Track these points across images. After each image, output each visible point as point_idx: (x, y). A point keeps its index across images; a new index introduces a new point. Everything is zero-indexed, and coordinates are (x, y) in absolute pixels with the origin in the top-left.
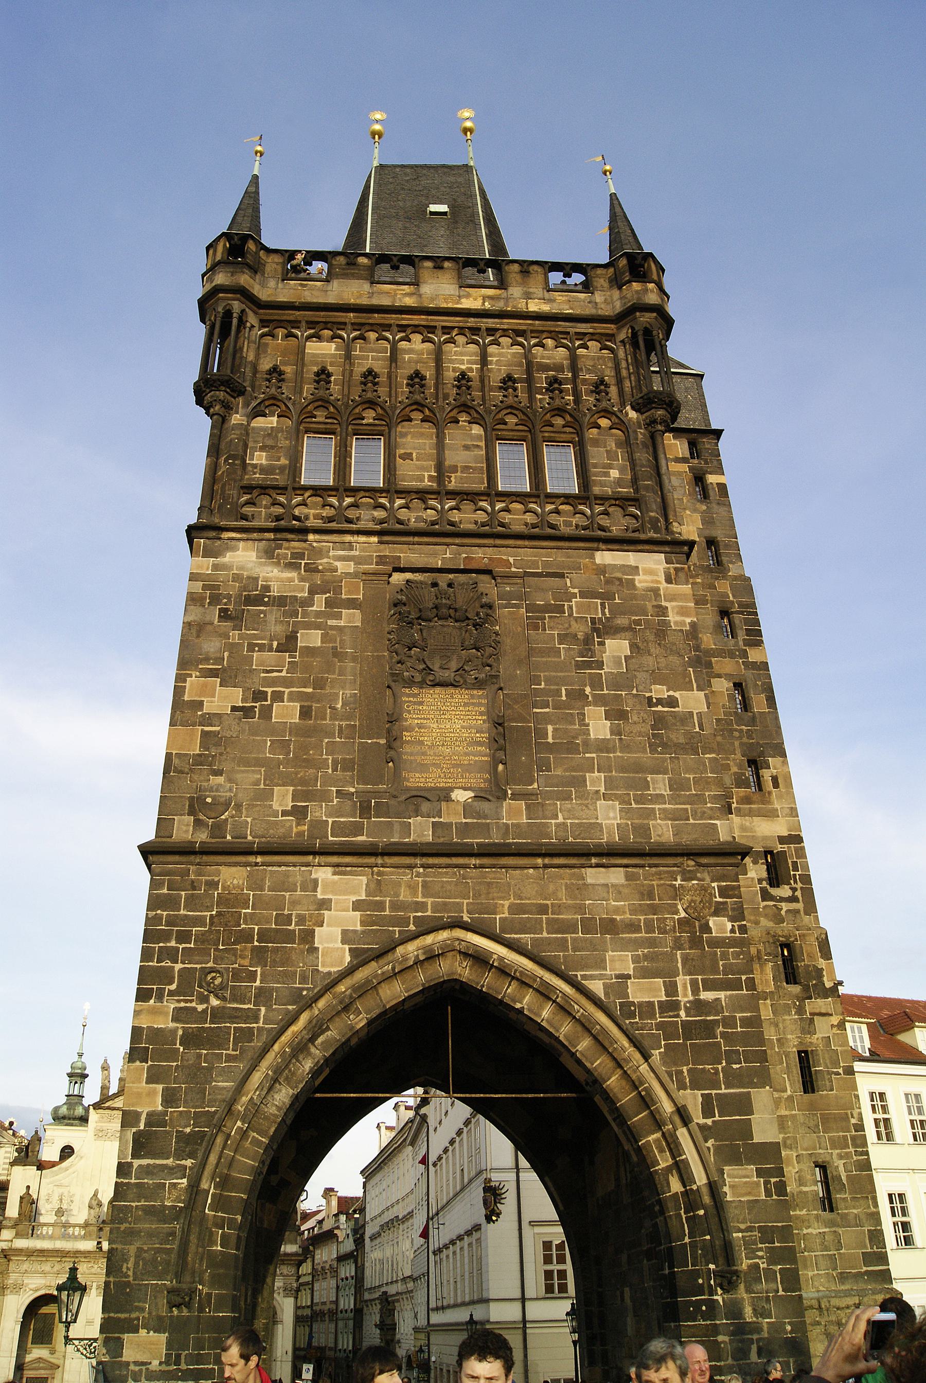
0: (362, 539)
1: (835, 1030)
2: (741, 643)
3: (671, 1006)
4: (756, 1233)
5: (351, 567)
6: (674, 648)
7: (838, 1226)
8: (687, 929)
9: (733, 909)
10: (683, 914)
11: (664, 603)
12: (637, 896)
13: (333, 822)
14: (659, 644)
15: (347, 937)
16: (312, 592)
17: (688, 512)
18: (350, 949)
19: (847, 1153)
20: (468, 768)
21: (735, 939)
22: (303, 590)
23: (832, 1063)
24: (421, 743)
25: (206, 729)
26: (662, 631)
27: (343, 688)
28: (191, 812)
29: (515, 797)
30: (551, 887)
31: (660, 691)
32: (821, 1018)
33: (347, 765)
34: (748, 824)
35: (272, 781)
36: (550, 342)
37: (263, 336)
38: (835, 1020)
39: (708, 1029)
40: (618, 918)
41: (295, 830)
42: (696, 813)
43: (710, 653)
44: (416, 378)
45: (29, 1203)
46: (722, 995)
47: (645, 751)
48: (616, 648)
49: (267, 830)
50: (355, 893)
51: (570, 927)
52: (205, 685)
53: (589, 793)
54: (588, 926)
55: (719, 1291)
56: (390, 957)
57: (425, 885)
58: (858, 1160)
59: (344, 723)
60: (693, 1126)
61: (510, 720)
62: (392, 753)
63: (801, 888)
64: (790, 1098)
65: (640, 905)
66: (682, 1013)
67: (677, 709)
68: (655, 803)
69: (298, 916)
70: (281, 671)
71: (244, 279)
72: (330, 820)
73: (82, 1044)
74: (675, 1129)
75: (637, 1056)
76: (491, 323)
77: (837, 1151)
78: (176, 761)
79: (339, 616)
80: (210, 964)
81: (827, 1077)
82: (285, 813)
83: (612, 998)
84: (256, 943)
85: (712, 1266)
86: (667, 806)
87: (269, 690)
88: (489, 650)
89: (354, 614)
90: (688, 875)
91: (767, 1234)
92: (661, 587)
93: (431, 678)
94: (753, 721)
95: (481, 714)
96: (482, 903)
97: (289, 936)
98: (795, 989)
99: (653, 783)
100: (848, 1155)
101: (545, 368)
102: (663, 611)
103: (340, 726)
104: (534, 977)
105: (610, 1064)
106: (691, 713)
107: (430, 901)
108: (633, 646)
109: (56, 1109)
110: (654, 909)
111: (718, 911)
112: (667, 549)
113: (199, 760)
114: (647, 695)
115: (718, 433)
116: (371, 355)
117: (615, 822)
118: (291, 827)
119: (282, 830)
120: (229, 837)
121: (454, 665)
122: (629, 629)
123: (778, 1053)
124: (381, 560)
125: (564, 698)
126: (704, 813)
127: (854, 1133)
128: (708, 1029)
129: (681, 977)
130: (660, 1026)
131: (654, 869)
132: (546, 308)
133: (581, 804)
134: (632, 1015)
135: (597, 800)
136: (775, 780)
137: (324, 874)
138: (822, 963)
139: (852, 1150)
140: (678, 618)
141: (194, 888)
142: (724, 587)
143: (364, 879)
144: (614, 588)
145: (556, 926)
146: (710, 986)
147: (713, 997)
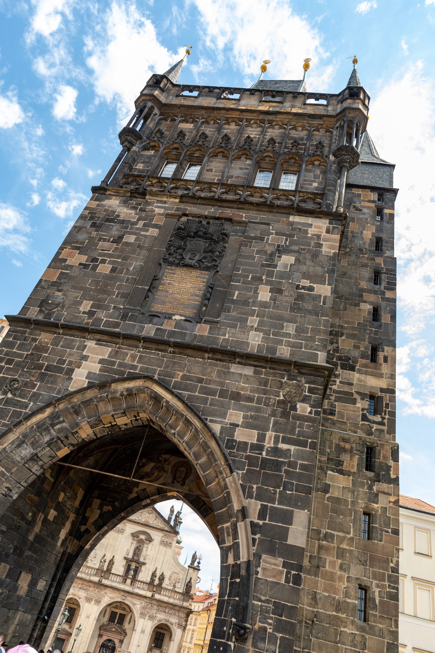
0: (172, 200)
1: (391, 504)
2: (382, 288)
3: (259, 448)
4: (271, 606)
5: (162, 211)
6: (321, 263)
7: (366, 633)
8: (282, 406)
9: (314, 401)
10: (282, 398)
11: (321, 242)
12: (257, 384)
13: (106, 320)
14: (312, 261)
15: (89, 375)
16: (139, 220)
17: (369, 225)
18: (89, 382)
19: (382, 585)
21: (310, 418)
22: (135, 218)
23: (385, 524)
24: (167, 291)
25: (63, 271)
26: (315, 255)
27: (136, 261)
28: (40, 306)
29: (206, 322)
30: (209, 370)
31: (306, 283)
32: (383, 495)
33: (124, 296)
34: (363, 378)
35: (84, 297)
37: (161, 119)
38: (392, 499)
39: (277, 465)
40: (242, 393)
41: (86, 321)
42: (307, 345)
43: (362, 290)
46: (292, 448)
47: (287, 311)
48: (287, 260)
49: (72, 319)
50: (102, 355)
51: (213, 393)
52: (71, 253)
53: (247, 326)
54: (223, 394)
55: (234, 640)
56: (107, 389)
57: (141, 357)
58: (390, 592)
59: (130, 277)
60: (248, 520)
61: (217, 287)
62: (149, 294)
63: (388, 418)
64: (352, 539)
65: (258, 388)
66: (264, 453)
67: (312, 293)
68: (284, 337)
69: (69, 361)
70: (109, 251)
72: (105, 319)
74: (237, 521)
75: (228, 471)
76: (271, 117)
77: (376, 582)
78: (43, 283)
79: (147, 230)
80: (16, 377)
81: (379, 532)
82: (84, 313)
83: (224, 435)
84: (43, 371)
85: (234, 620)
86: (291, 340)
87: (100, 258)
88: (217, 253)
89: (155, 231)
90: (292, 377)
91: (279, 609)
92: (322, 234)
93: (182, 262)
95: (203, 282)
96: (167, 372)
97: (60, 370)
98: (371, 474)
99: (286, 327)
100: (383, 587)
102: (320, 246)
103: (128, 278)
104: (182, 415)
105: (214, 475)
106: (320, 296)
107: (140, 365)
108: (297, 260)
110: (265, 392)
111: (304, 400)
112: (331, 218)
113: (54, 284)
114: (297, 283)
117: (257, 343)
118: (84, 320)
119: (79, 320)
120: (52, 320)
121: (197, 258)
122: (298, 252)
123: (350, 509)
124: (178, 209)
125: (249, 279)
126: (312, 346)
127: (390, 573)
128: (277, 465)
129: (270, 432)
130: (247, 457)
131: (272, 371)
132: (301, 111)
133: (241, 331)
134: (233, 447)
135: (251, 330)
136: (386, 359)
137: (91, 344)
138: (391, 463)
139: (387, 583)
140: (327, 250)
141: (25, 340)
142: (380, 260)
143: (110, 349)
144: (295, 233)
145: (205, 391)
146: (285, 441)
147: (286, 448)
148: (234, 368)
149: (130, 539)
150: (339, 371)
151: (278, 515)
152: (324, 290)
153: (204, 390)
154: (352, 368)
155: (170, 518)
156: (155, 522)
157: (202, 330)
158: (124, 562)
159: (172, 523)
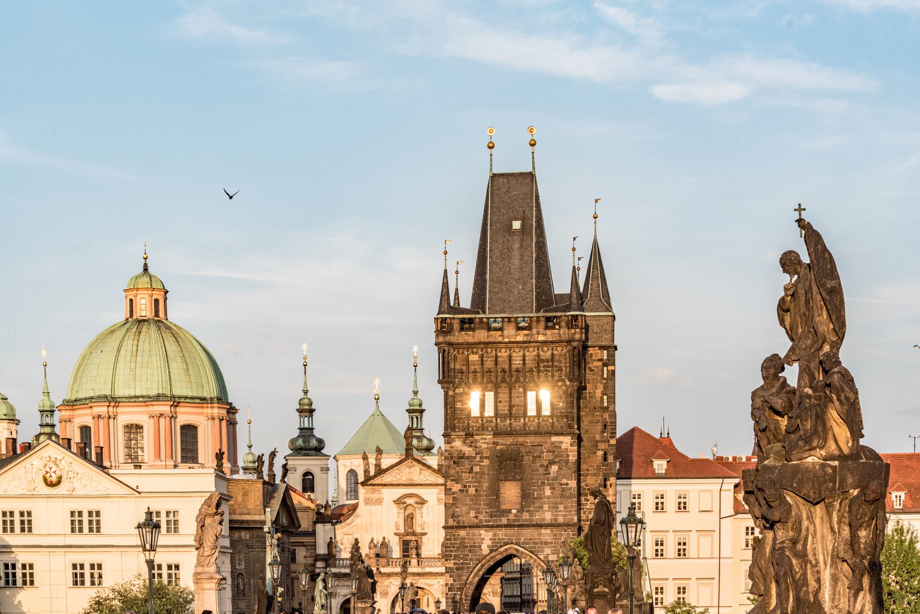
20: (516, 504)
26: (567, 462)
33: (487, 505)
36: (545, 349)
43: (597, 442)
45: (331, 545)
48: (554, 468)
73: (305, 383)
101: (543, 361)
102: (568, 456)
108: (559, 468)
109: (293, 441)
113: (453, 504)
124: (494, 443)
137: (483, 532)
142: (606, 416)
148: (543, 531)
149: (394, 507)
150: (589, 497)
156: (422, 476)
157: (526, 516)
158: (396, 539)
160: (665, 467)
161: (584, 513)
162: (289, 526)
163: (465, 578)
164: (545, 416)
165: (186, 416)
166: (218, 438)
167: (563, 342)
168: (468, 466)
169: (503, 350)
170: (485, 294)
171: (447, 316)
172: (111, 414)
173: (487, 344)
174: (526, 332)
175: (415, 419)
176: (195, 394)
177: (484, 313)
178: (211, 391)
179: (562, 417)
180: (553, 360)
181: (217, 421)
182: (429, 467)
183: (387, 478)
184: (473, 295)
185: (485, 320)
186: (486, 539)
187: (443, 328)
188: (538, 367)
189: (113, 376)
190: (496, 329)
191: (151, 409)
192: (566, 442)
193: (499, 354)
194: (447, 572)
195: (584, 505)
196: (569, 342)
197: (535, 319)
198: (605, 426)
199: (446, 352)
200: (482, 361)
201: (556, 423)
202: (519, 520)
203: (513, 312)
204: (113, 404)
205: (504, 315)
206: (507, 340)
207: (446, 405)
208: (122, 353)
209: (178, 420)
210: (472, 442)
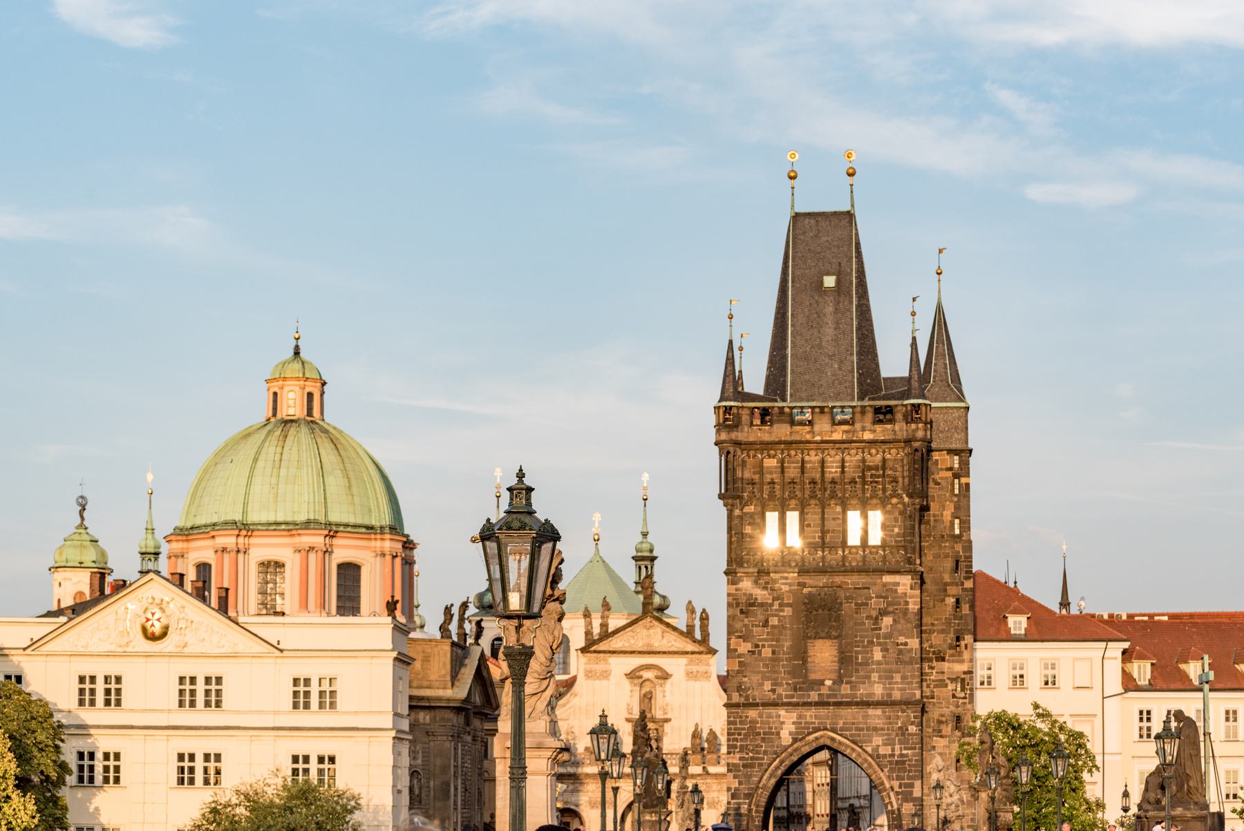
3: (893, 755)
15: (790, 733)
16: (774, 600)
20: (831, 672)
26: (905, 612)
31: (902, 639)
33: (789, 673)
36: (873, 451)
39: (904, 762)
43: (946, 584)
44: (813, 482)
48: (887, 621)
51: (862, 729)
71: (735, 435)
94: (961, 618)
98: (958, 733)
101: (870, 468)
102: (907, 603)
111: (912, 723)
113: (738, 672)
115: (971, 451)
116: (793, 472)
124: (799, 584)
128: (904, 762)
137: (782, 712)
142: (959, 547)
148: (871, 712)
149: (626, 684)
150: (935, 664)
151: (907, 785)
152: (914, 643)
153: (857, 729)
154: (943, 659)
155: (691, 628)
156: (665, 641)
157: (845, 689)
159: (698, 635)
160: (1024, 624)
161: (928, 686)
162: (483, 706)
163: (756, 779)
164: (874, 547)
165: (344, 551)
166: (389, 582)
167: (899, 441)
168: (762, 618)
169: (813, 453)
170: (785, 376)
171: (732, 403)
172: (241, 547)
173: (791, 443)
174: (846, 427)
175: (643, 570)
176: (359, 521)
177: (784, 400)
178: (382, 517)
179: (898, 548)
180: (884, 468)
181: (388, 558)
182: (675, 629)
183: (616, 643)
184: (768, 377)
185: (787, 410)
186: (787, 723)
187: (727, 420)
188: (863, 477)
189: (247, 494)
190: (801, 423)
191: (297, 540)
192: (904, 582)
193: (807, 458)
194: (729, 771)
195: (927, 674)
196: (908, 442)
197: (859, 409)
198: (957, 562)
199: (731, 452)
200: (783, 467)
201: (890, 557)
202: (835, 696)
203: (825, 400)
204: (244, 532)
205: (814, 404)
206: (818, 438)
207: (730, 529)
208: (260, 464)
209: (334, 556)
210: (767, 583)
